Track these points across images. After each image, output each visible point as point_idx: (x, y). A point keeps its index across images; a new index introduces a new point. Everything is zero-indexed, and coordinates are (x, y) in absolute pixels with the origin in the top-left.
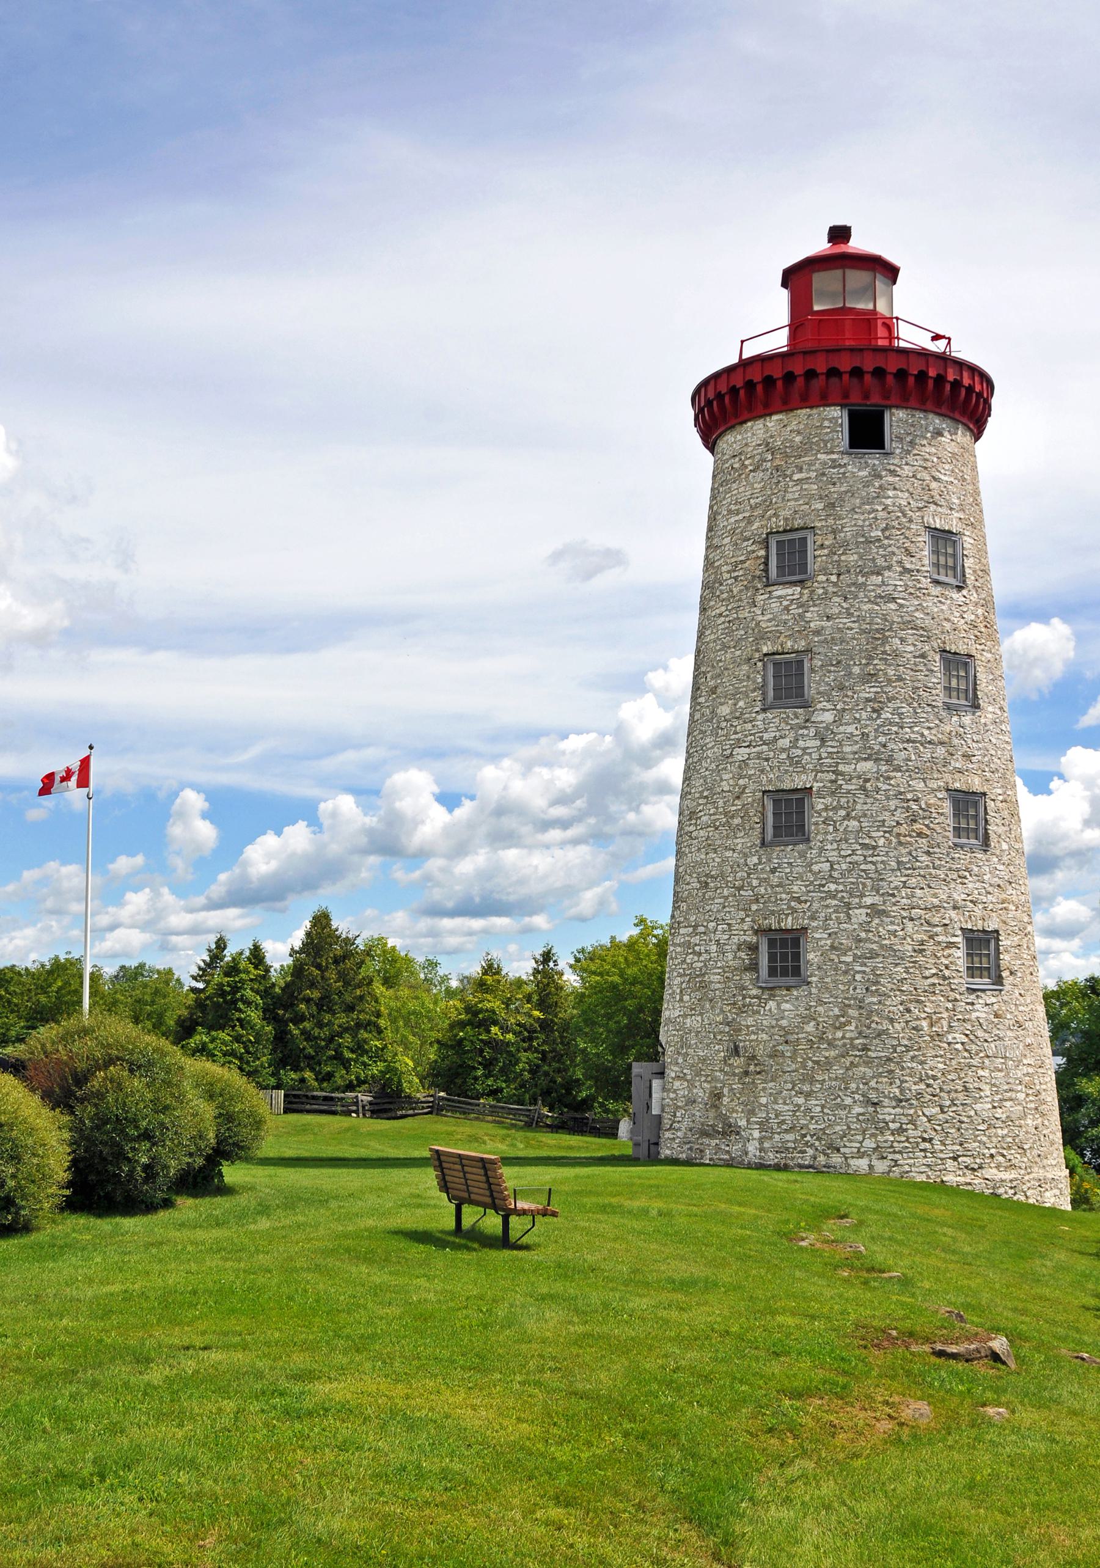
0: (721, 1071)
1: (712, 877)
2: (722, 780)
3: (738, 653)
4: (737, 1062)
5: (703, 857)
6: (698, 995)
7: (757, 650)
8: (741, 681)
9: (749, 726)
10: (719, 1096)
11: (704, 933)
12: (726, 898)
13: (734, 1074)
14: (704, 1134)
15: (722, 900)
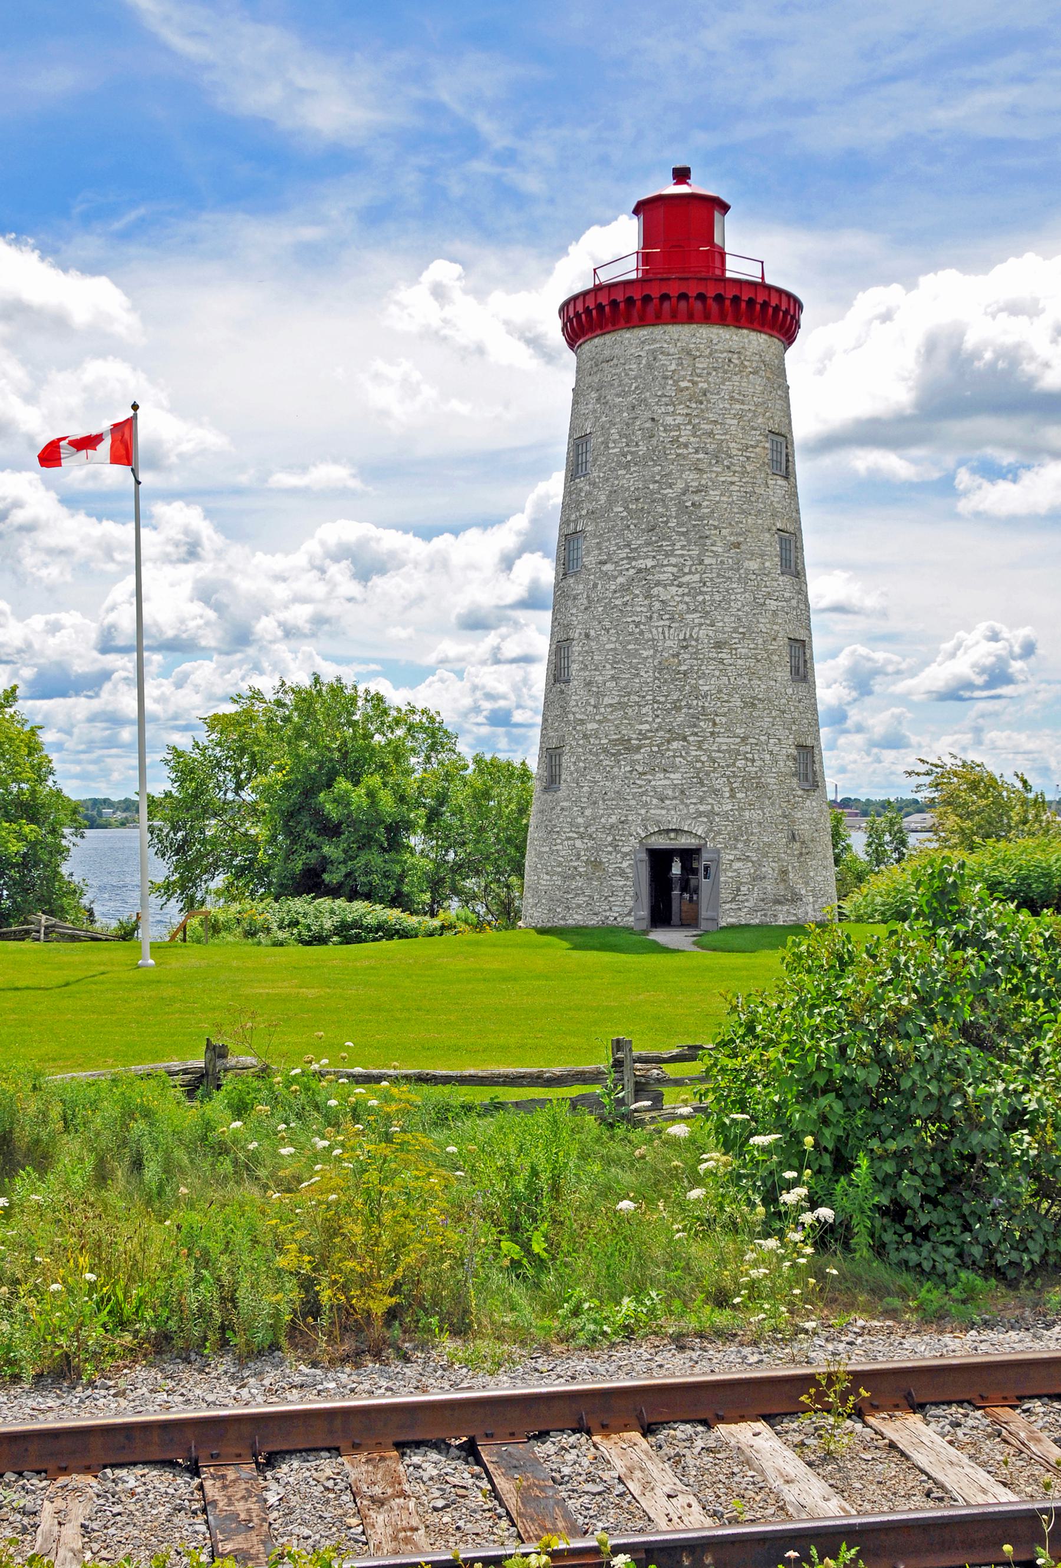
0: (785, 853)
1: (759, 699)
2: (758, 622)
3: (760, 522)
4: (797, 845)
5: (746, 682)
6: (757, 793)
7: (774, 524)
8: (767, 546)
9: (775, 584)
10: (785, 872)
11: (756, 744)
12: (774, 718)
13: (794, 855)
14: (777, 902)
15: (771, 720)
